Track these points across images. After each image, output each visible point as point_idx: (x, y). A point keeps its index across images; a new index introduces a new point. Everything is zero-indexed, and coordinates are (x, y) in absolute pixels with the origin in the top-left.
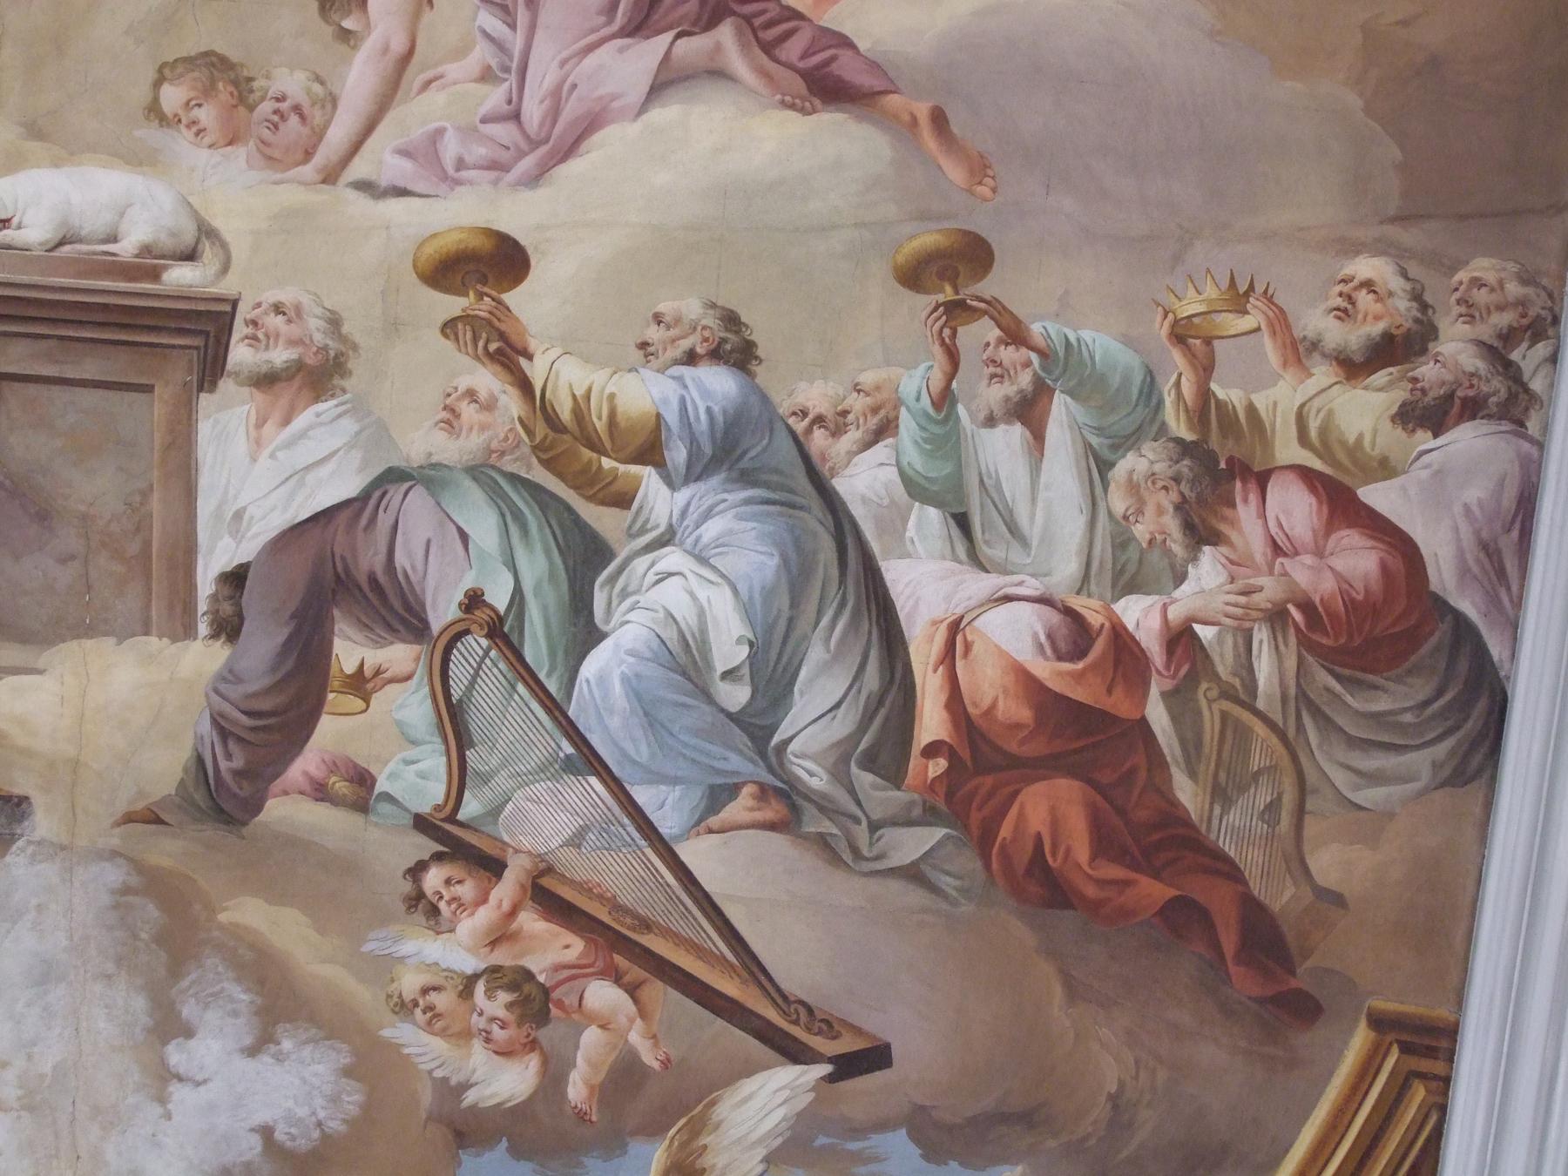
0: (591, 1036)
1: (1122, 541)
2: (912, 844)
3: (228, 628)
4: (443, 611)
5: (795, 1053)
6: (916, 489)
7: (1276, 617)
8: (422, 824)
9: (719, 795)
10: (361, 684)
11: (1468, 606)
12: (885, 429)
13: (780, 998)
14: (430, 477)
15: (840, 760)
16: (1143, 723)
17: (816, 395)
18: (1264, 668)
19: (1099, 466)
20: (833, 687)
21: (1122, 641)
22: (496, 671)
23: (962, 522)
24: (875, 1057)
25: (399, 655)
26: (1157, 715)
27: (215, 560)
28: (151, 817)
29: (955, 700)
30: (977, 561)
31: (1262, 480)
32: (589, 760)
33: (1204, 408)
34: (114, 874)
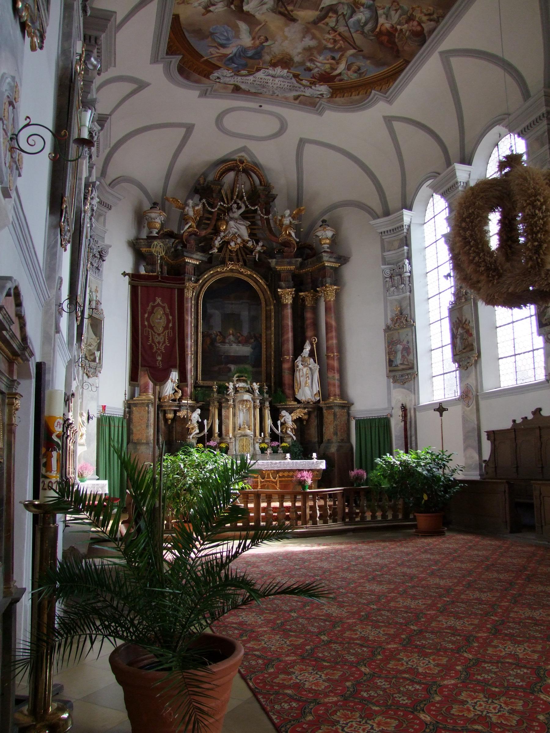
0: (339, 45)
1: (400, 22)
2: (373, 38)
3: (321, 11)
4: (340, 13)
5: (354, 48)
6: (384, 13)
7: (410, 31)
8: (331, 28)
9: (357, 31)
10: (330, 17)
11: (426, 35)
12: (384, 8)
13: (356, 46)
14: (343, 4)
15: (369, 31)
16: (395, 35)
17: (379, 5)
18: (407, 34)
19: (400, 16)
20: (371, 26)
21: (396, 29)
22: (342, 19)
23: (387, 17)
24: (362, 51)
25: (335, 16)
26: (397, 35)
27: (322, 5)
28: (309, 23)
29: (380, 29)
30: (387, 20)
31: (414, 21)
32: (347, 26)
33: (412, 14)
34: (304, 26)
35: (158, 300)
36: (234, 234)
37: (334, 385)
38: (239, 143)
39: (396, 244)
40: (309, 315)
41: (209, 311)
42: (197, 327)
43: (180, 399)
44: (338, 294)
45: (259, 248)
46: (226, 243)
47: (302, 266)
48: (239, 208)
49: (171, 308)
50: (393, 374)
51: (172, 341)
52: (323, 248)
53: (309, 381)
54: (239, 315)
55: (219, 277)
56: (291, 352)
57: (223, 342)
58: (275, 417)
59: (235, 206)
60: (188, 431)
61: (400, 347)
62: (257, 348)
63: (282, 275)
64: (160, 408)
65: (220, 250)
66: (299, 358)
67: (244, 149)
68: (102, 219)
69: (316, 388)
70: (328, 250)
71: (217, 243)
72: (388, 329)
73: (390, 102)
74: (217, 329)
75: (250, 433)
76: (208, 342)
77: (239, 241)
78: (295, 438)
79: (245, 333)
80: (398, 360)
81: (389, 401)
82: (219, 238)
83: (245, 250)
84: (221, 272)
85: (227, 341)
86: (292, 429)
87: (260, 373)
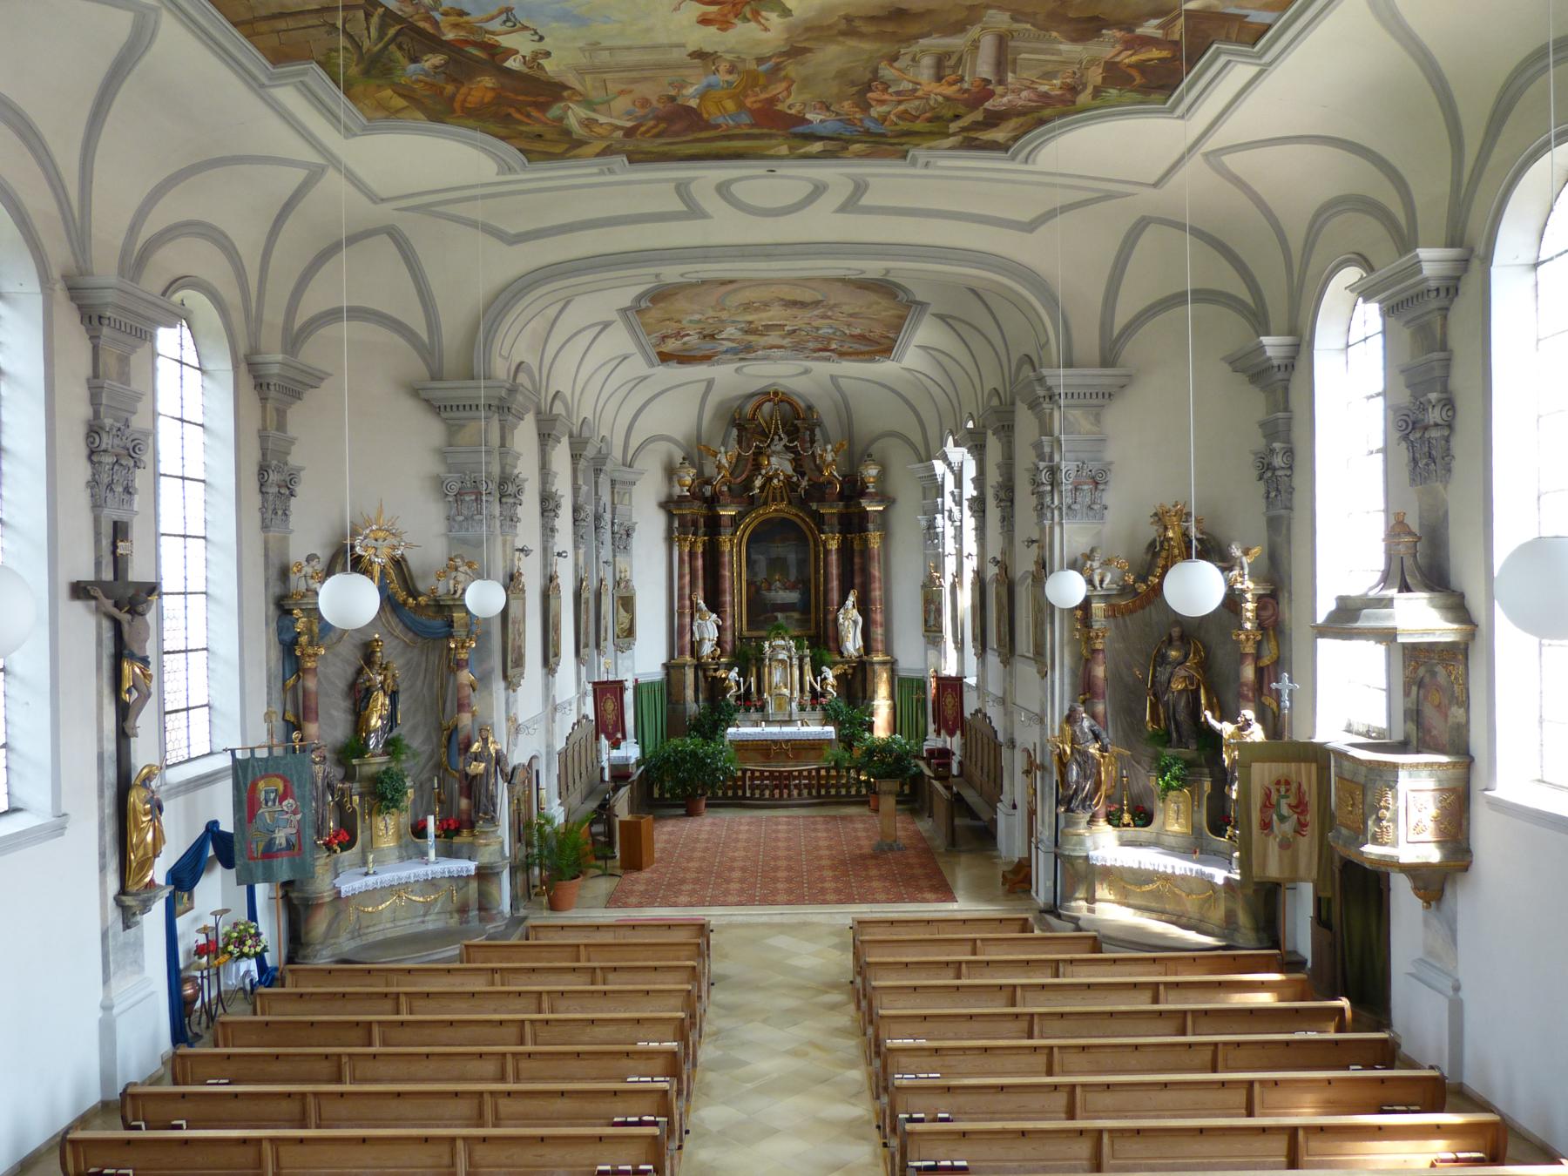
35: (608, 695)
36: (777, 470)
37: (876, 640)
38: (771, 381)
39: (934, 491)
40: (857, 560)
41: (754, 557)
42: (740, 575)
43: (719, 658)
44: (886, 539)
45: (804, 483)
46: (769, 479)
47: (847, 506)
48: (781, 439)
49: (616, 698)
50: (927, 634)
51: (618, 718)
52: (868, 487)
53: (851, 636)
54: (785, 559)
55: (760, 519)
56: (835, 602)
57: (769, 589)
58: (817, 672)
59: (777, 438)
60: (727, 689)
61: (933, 607)
62: (805, 594)
63: (826, 517)
64: (700, 667)
65: (762, 488)
66: (842, 611)
67: (774, 384)
68: (627, 496)
69: (860, 642)
70: (873, 490)
71: (758, 482)
72: (924, 586)
73: (900, 362)
74: (762, 575)
75: (786, 692)
76: (753, 589)
77: (782, 478)
78: (835, 694)
79: (793, 578)
80: (932, 622)
81: (926, 660)
82: (760, 477)
83: (790, 485)
84: (762, 515)
85: (773, 588)
86: (833, 686)
87: (808, 621)
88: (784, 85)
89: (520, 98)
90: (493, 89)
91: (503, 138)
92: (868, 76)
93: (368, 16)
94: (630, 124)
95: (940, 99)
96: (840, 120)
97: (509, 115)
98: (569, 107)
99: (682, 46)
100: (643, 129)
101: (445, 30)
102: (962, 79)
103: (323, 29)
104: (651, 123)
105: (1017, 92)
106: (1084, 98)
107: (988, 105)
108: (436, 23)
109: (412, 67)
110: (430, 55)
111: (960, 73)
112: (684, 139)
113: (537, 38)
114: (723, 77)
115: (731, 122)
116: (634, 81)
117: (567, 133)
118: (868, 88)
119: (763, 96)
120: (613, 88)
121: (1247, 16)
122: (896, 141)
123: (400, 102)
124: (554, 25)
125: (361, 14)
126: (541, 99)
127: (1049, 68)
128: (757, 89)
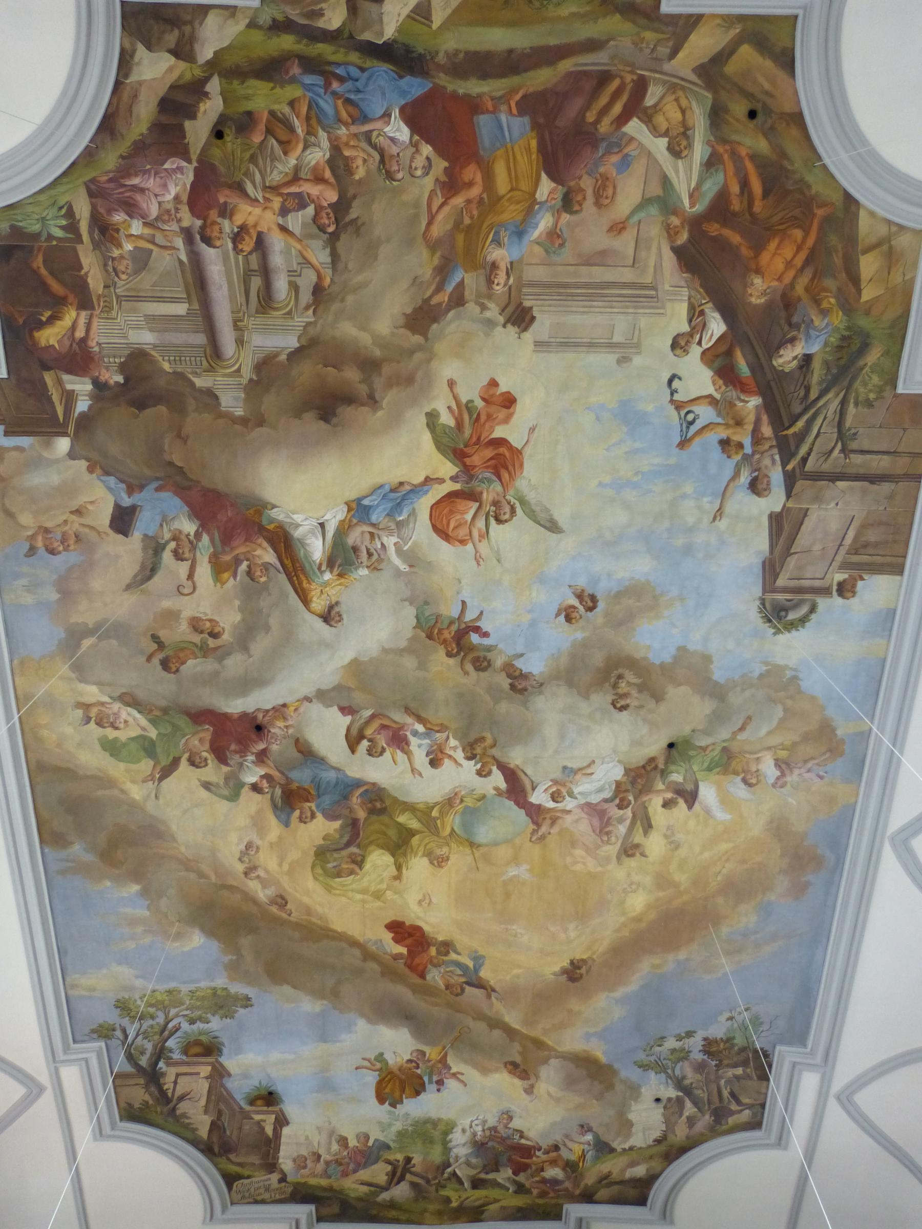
88: (437, 231)
89: (735, 238)
90: (758, 271)
91: (797, 119)
92: (341, 246)
93: (804, 460)
94: (634, 127)
95: (250, 188)
96: (365, 119)
97: (766, 194)
98: (691, 196)
99: (540, 345)
100: (617, 109)
101: (751, 418)
102: (237, 238)
103: (854, 445)
104: (605, 126)
105: (165, 215)
106: (83, 210)
107: (189, 177)
108: (756, 431)
109: (815, 348)
110: (787, 370)
111: (240, 257)
112: (567, 65)
113: (676, 384)
114: (500, 255)
115: (503, 118)
116: (600, 258)
117: (717, 115)
118: (341, 208)
119: (458, 201)
120: (625, 243)
121: (7, 434)
122: (287, 42)
123: (868, 265)
124: (650, 408)
125: (810, 466)
126: (714, 229)
127: (146, 281)
128: (467, 221)
